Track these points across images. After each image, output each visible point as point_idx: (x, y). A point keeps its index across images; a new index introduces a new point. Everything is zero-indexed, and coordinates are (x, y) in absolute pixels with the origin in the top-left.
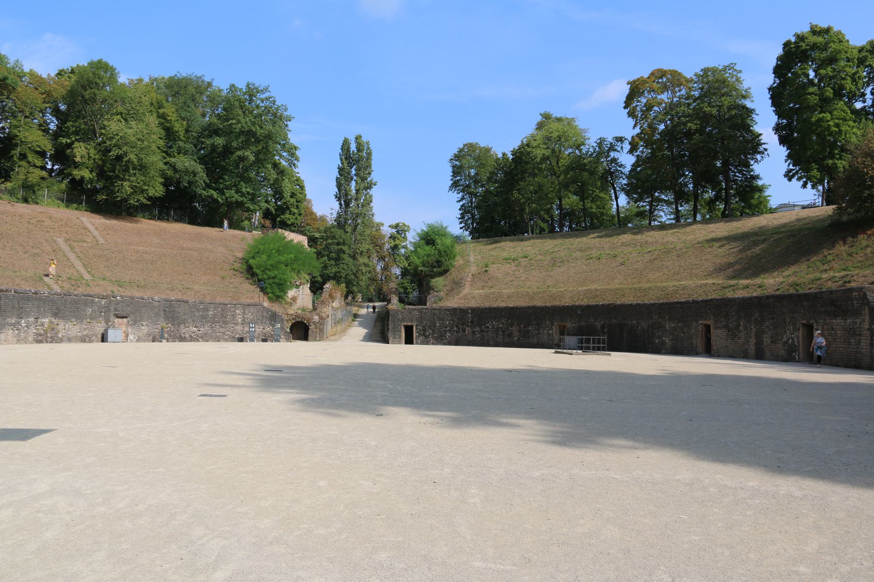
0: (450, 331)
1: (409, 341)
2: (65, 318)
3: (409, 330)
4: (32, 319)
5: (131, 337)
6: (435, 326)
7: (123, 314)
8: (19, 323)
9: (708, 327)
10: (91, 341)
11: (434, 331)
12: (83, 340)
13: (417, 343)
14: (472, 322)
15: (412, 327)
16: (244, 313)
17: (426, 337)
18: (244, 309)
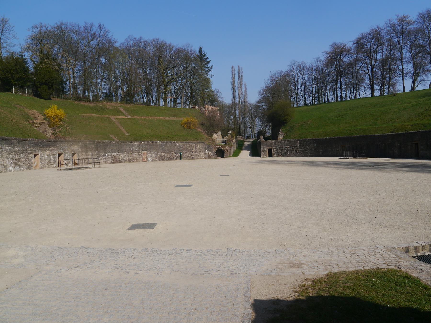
0: (290, 150)
1: (271, 156)
2: (122, 152)
3: (270, 151)
4: (110, 154)
5: (149, 159)
6: (282, 149)
7: (146, 149)
8: (105, 155)
9: (417, 144)
10: (133, 161)
11: (282, 151)
12: (130, 161)
13: (274, 157)
14: (300, 146)
15: (272, 149)
16: (196, 147)
17: (279, 154)
18: (196, 144)
